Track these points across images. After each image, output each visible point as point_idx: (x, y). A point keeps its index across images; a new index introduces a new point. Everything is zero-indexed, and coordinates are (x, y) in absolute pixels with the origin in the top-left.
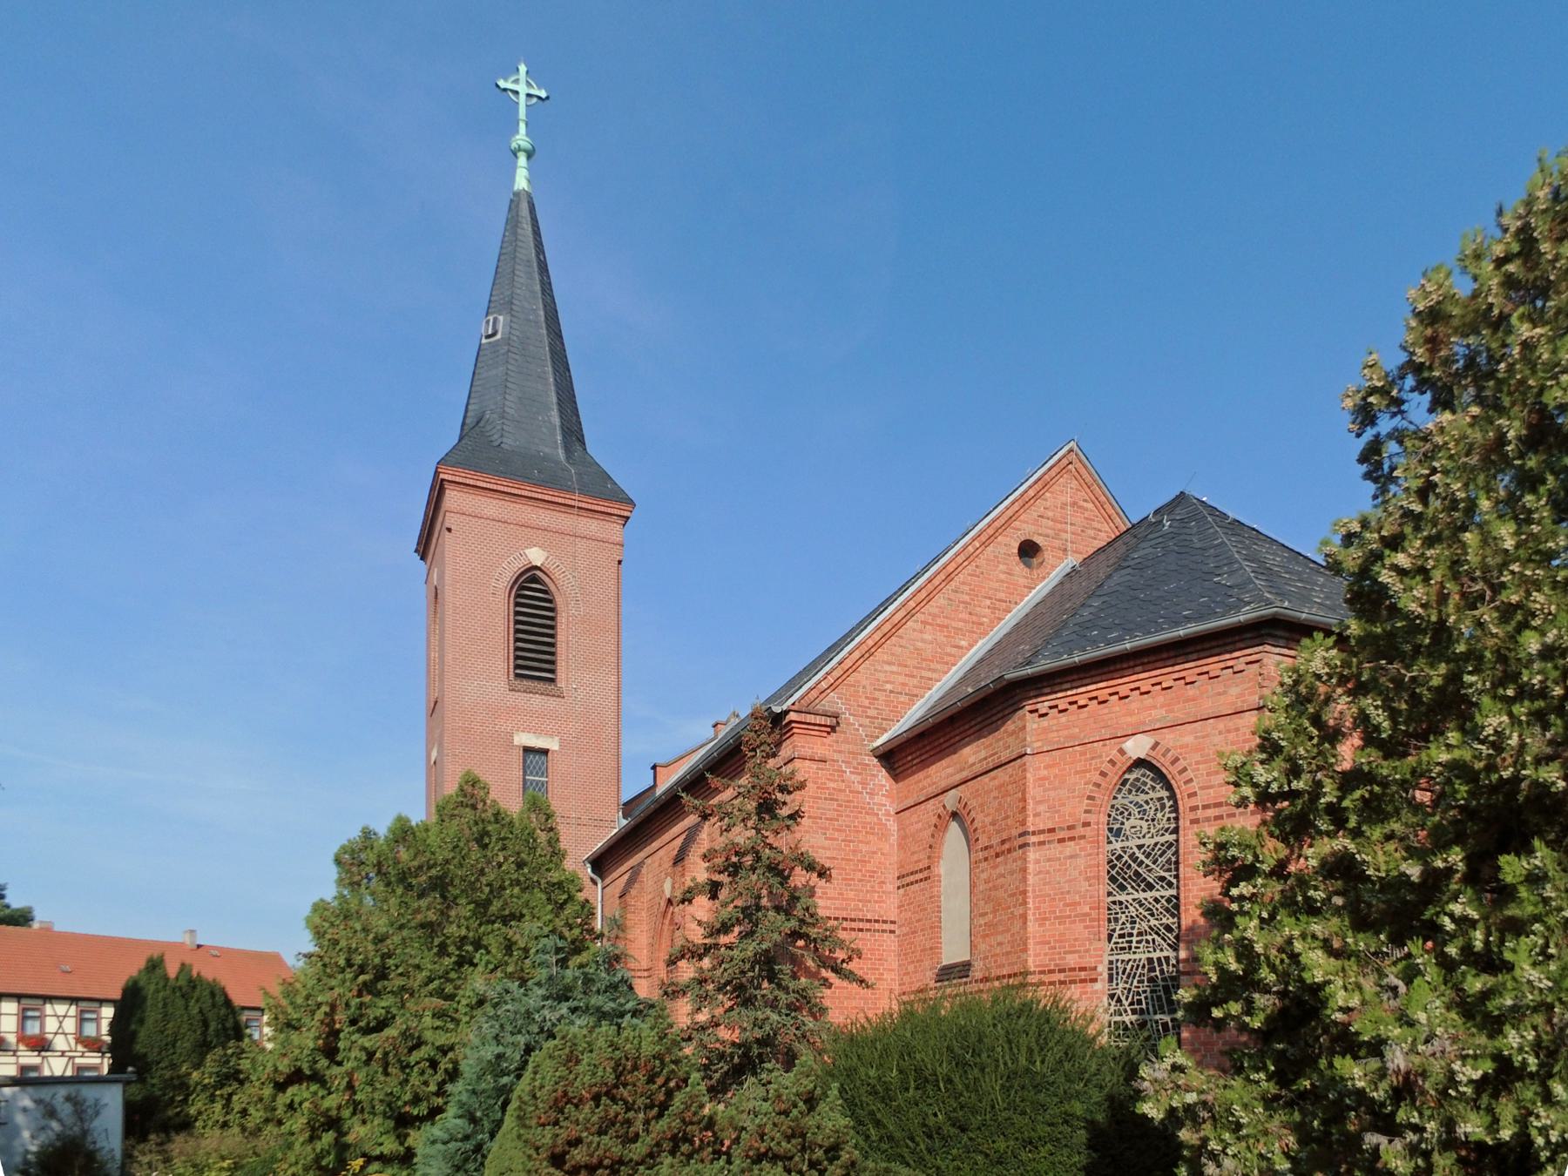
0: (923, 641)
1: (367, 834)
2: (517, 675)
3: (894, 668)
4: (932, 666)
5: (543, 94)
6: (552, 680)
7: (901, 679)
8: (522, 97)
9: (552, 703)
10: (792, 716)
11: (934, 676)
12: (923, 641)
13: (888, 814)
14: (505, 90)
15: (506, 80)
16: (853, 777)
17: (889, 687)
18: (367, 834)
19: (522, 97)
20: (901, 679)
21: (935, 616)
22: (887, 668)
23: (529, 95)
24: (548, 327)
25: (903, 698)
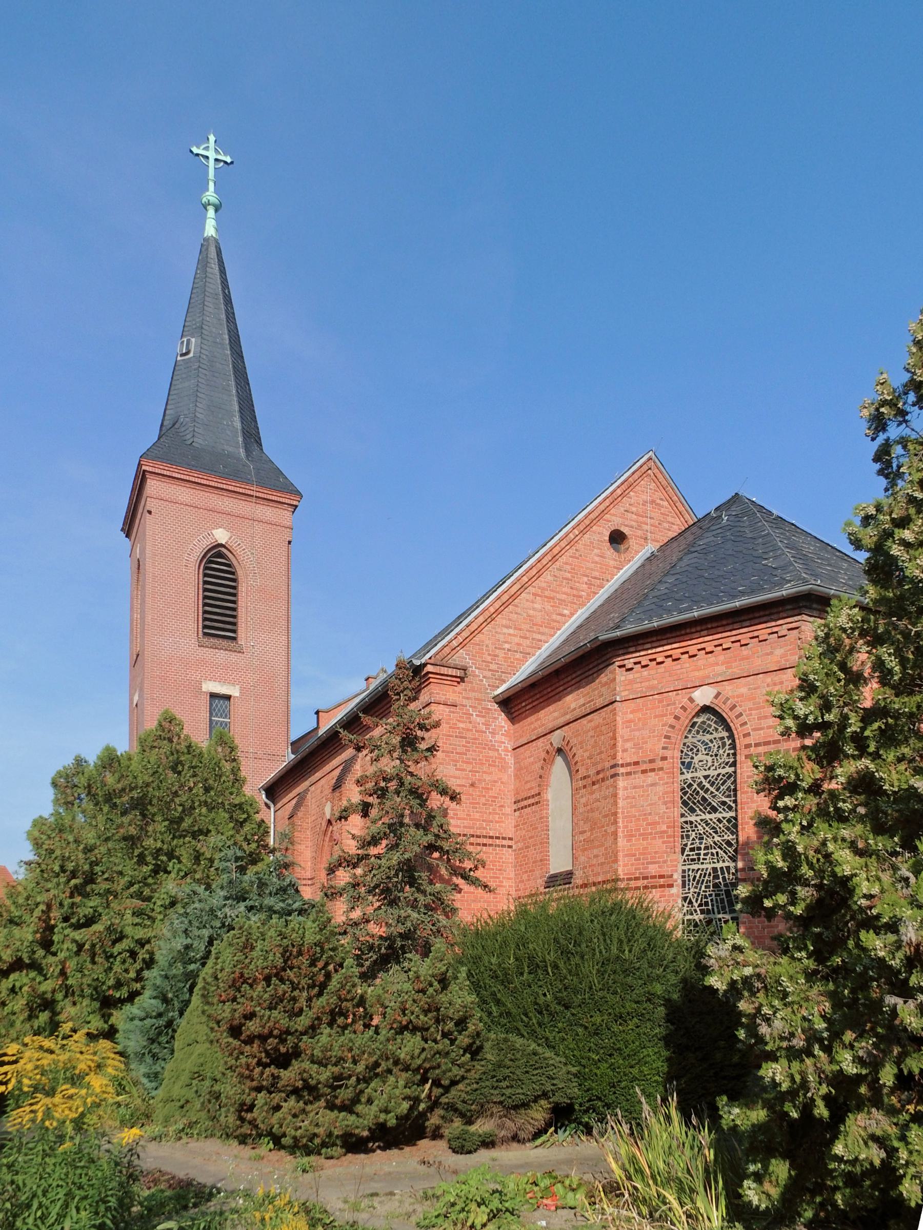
0: (534, 609)
1: (79, 762)
2: (205, 634)
3: (511, 631)
4: (542, 629)
5: (229, 160)
6: (234, 639)
7: (517, 640)
8: (211, 162)
9: (233, 657)
10: (430, 668)
11: (543, 638)
12: (534, 609)
13: (506, 750)
14: (197, 155)
15: (198, 147)
16: (478, 719)
17: (507, 646)
18: (79, 762)
19: (211, 162)
20: (517, 640)
21: (543, 589)
22: (505, 630)
23: (216, 160)
24: (232, 348)
25: (518, 656)
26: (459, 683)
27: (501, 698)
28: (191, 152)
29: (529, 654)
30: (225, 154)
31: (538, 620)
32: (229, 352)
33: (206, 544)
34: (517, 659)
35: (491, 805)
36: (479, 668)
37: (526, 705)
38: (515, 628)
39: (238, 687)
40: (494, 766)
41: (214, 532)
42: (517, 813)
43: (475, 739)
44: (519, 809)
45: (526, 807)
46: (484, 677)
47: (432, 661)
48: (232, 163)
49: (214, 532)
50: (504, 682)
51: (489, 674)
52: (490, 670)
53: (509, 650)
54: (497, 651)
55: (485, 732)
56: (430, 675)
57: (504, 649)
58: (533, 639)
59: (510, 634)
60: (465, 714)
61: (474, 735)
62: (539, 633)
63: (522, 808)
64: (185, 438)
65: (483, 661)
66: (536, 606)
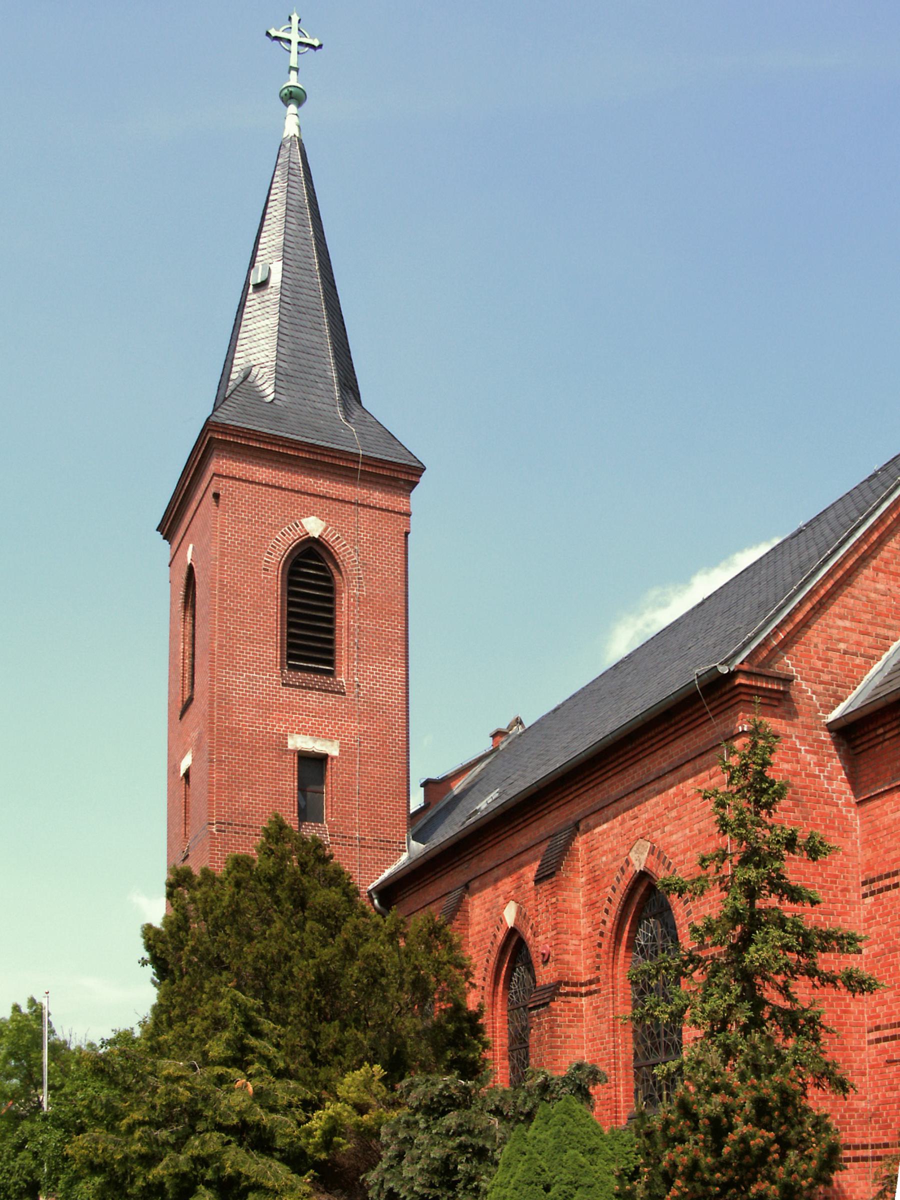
0: (876, 591)
1: (518, 722)
2: (292, 667)
3: (847, 624)
4: (890, 621)
5: (316, 43)
6: (330, 673)
7: (855, 637)
8: (294, 47)
9: (330, 700)
10: (741, 680)
11: (890, 633)
12: (876, 591)
13: (848, 804)
14: (277, 38)
15: (277, 30)
16: (809, 756)
17: (842, 646)
18: (518, 722)
19: (294, 47)
20: (855, 637)
21: (887, 562)
22: (840, 623)
23: (300, 43)
24: (323, 276)
25: (859, 661)
26: (779, 700)
27: (835, 726)
28: (268, 34)
29: (873, 658)
30: (312, 38)
31: (882, 608)
32: (319, 280)
33: (283, 543)
34: (858, 666)
35: (831, 889)
36: (806, 680)
37: (885, 733)
38: (853, 620)
39: (337, 743)
40: (833, 828)
41: (304, 521)
42: (869, 900)
43: (805, 787)
44: (872, 893)
45: (888, 888)
46: (814, 693)
47: (745, 667)
48: (320, 46)
49: (304, 521)
50: (842, 700)
51: (820, 688)
52: (821, 683)
53: (846, 652)
54: (830, 653)
55: (819, 777)
56: (743, 690)
57: (839, 651)
58: (877, 636)
59: (845, 628)
60: (790, 749)
61: (803, 780)
62: (885, 627)
63: (880, 891)
64: (263, 394)
65: (812, 669)
66: (879, 586)
